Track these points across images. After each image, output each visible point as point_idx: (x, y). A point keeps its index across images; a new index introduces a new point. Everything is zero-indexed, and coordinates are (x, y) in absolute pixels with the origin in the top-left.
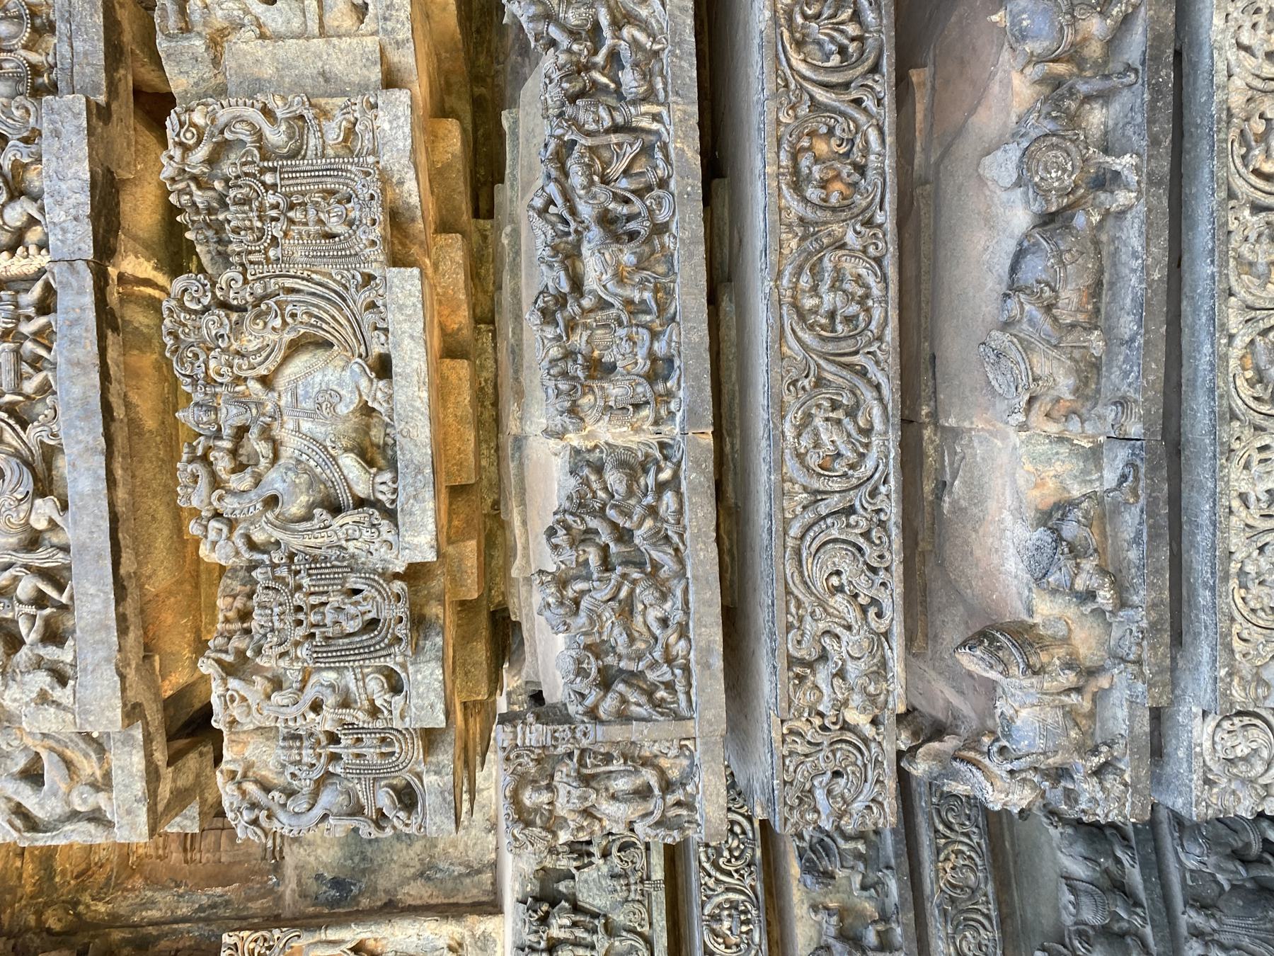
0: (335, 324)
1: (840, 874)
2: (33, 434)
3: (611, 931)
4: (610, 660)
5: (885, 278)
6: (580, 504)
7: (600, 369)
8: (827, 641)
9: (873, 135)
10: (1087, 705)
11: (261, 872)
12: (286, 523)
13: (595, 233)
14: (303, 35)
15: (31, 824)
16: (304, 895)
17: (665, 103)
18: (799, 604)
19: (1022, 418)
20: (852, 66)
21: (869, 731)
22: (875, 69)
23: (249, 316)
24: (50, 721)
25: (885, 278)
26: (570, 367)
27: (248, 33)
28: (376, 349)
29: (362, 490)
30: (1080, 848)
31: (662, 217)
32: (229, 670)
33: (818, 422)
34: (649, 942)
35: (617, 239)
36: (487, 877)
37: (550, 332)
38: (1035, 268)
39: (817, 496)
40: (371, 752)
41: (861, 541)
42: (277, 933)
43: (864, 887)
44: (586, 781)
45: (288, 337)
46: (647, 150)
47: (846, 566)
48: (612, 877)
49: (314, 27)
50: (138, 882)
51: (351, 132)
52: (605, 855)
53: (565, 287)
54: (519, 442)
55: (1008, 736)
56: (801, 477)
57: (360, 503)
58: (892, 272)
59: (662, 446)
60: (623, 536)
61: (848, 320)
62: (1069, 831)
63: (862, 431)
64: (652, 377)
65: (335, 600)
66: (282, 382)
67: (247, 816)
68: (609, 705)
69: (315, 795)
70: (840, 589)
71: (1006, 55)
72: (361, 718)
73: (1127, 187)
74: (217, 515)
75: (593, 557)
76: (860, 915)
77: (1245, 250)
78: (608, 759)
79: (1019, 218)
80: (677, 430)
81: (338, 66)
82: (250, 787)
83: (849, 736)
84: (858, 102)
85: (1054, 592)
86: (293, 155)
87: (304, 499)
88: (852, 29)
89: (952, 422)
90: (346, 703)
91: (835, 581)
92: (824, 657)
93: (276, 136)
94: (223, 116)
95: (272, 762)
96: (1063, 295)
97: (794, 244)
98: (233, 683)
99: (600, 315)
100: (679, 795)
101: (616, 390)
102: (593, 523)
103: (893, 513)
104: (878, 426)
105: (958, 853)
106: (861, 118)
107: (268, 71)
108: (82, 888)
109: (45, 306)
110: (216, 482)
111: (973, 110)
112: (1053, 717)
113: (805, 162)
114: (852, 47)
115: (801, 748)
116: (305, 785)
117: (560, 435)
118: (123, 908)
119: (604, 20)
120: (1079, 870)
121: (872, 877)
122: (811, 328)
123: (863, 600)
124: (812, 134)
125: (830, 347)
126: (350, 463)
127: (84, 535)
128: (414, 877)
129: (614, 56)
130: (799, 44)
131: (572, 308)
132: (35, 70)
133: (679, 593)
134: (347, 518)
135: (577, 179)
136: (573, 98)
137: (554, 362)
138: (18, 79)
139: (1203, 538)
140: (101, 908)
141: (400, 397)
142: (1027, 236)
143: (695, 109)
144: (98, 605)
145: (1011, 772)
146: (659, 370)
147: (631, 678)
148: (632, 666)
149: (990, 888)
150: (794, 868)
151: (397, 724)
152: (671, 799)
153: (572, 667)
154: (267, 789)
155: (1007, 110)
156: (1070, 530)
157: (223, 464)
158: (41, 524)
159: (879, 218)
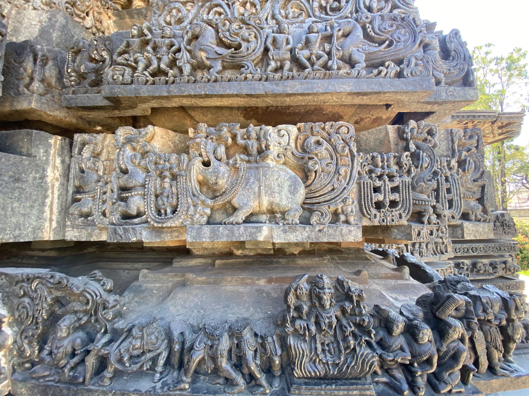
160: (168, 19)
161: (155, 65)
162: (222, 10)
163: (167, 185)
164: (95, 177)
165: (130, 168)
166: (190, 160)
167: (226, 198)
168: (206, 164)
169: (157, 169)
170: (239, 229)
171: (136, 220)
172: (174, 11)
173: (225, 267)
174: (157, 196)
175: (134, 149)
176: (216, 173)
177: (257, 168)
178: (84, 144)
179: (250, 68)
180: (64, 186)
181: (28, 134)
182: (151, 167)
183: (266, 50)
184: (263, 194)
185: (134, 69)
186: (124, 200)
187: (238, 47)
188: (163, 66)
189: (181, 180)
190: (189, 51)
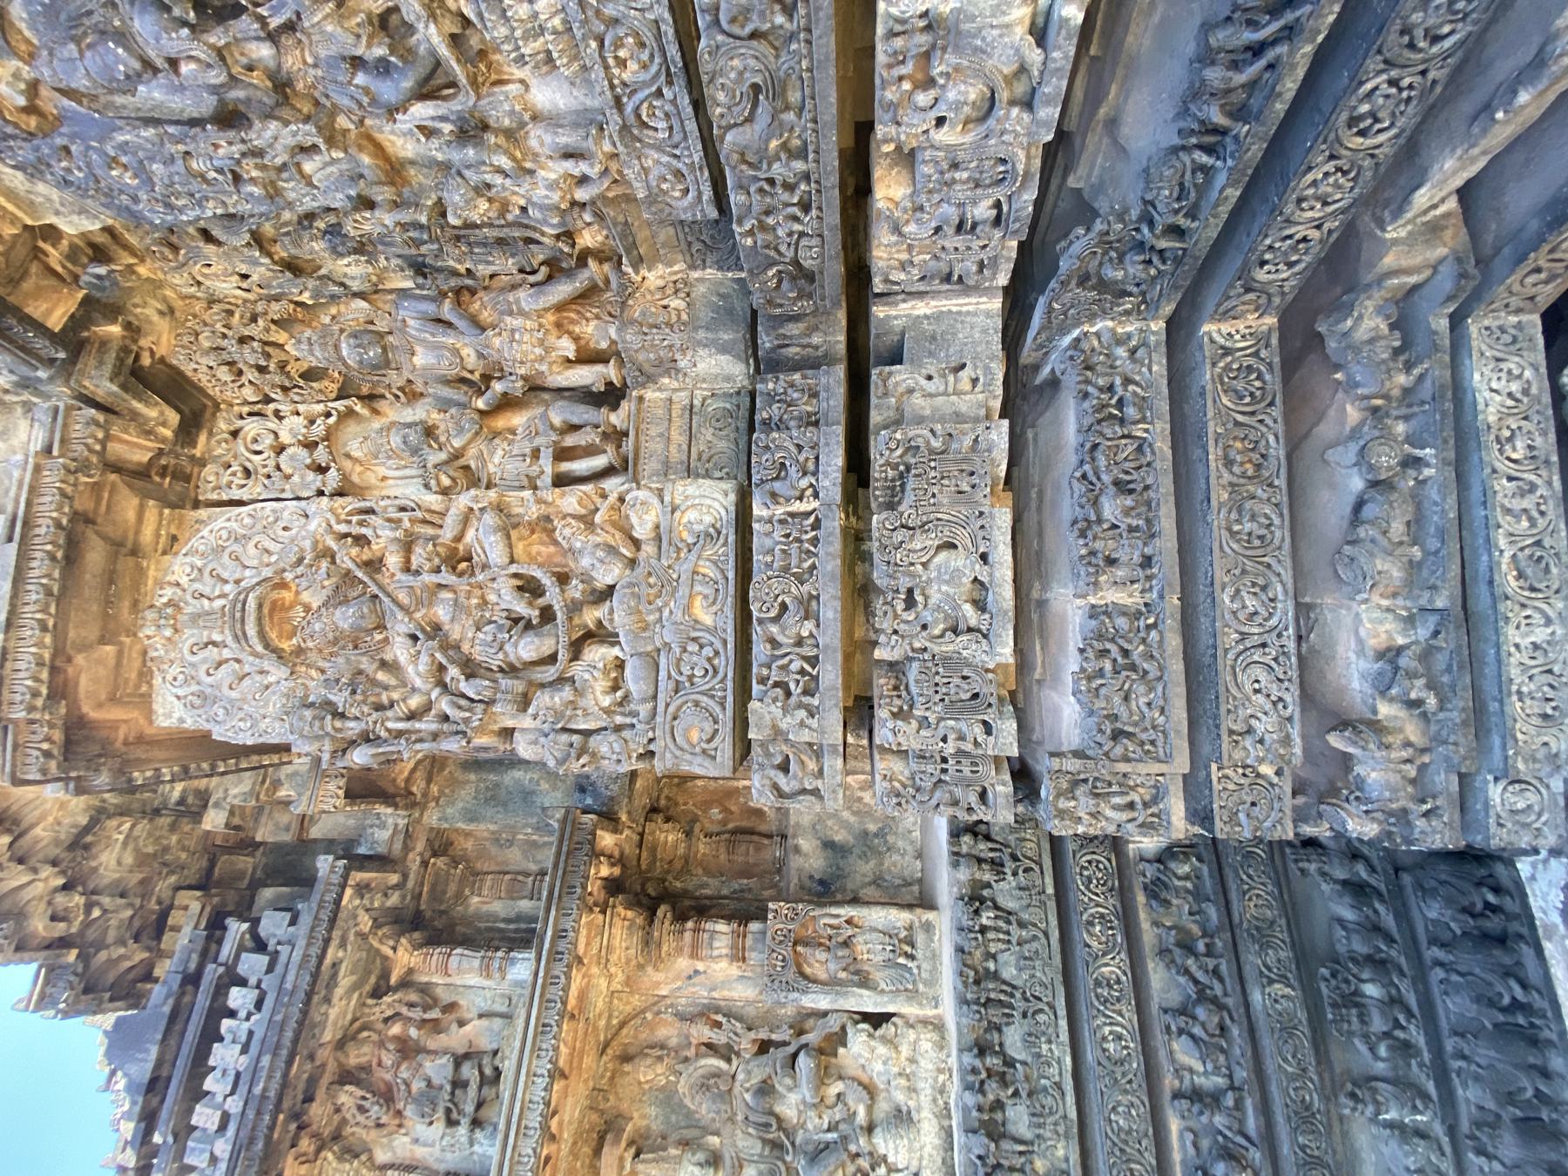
0: (962, 537)
1: (1175, 901)
2: (805, 588)
3: (1022, 925)
4: (1119, 725)
5: (1281, 515)
6: (1100, 637)
7: (1111, 562)
8: (1253, 722)
9: (1271, 439)
10: (1413, 773)
11: (769, 872)
12: (933, 638)
13: (1112, 490)
14: (945, 394)
15: (781, 794)
16: (802, 888)
17: (1151, 423)
18: (1235, 698)
19: (1365, 596)
20: (1259, 402)
21: (1275, 780)
22: (1271, 404)
23: (918, 531)
24: (806, 736)
25: (1281, 515)
26: (1094, 561)
27: (917, 394)
28: (982, 550)
29: (973, 623)
30: (1348, 899)
31: (1149, 481)
32: (895, 715)
33: (1244, 593)
34: (1046, 934)
35: (1123, 492)
36: (916, 888)
37: (1081, 542)
38: (1369, 511)
39: (1244, 636)
40: (967, 770)
41: (1273, 664)
42: (800, 906)
43: (1191, 914)
44: (1097, 795)
45: (937, 543)
46: (1140, 449)
47: (1263, 676)
48: (1020, 889)
49: (950, 390)
50: (700, 871)
51: (976, 440)
52: (1015, 874)
53: (1093, 517)
54: (1042, 604)
55: (1361, 789)
56: (1234, 624)
57: (970, 630)
58: (1286, 512)
59: (1146, 605)
60: (1126, 653)
61: (1261, 538)
62: (1338, 887)
63: (1272, 600)
64: (1142, 566)
65: (957, 681)
66: (932, 566)
67: (895, 800)
68: (1118, 750)
69: (932, 791)
70: (1257, 691)
71: (1340, 395)
72: (969, 747)
73: (1428, 465)
74: (895, 632)
75: (1108, 666)
76: (1188, 932)
77: (1506, 502)
78: (1110, 785)
79: (1357, 484)
80: (1155, 595)
81: (964, 409)
82: (896, 784)
83: (1260, 781)
84: (1261, 421)
85: (1392, 700)
86: (942, 453)
87: (942, 626)
88: (1257, 384)
89: (1307, 599)
90: (962, 738)
91: (1256, 686)
92: (1250, 731)
93: (936, 444)
94: (911, 434)
95: (907, 773)
96: (1394, 525)
97: (1226, 496)
98: (899, 723)
99: (1111, 533)
100: (1154, 810)
101: (1120, 573)
102: (1108, 646)
103: (1291, 646)
104: (1280, 597)
105: (1258, 896)
106: (1264, 430)
107: (928, 412)
108: (668, 872)
109: (816, 526)
110: (896, 616)
111: (1316, 424)
112: (1394, 778)
113: (1232, 454)
114: (1258, 393)
115: (1231, 787)
116: (928, 784)
117: (1084, 596)
118: (690, 887)
119: (1118, 381)
120: (1349, 915)
121: (1195, 908)
122: (1238, 541)
123: (1274, 698)
124: (1235, 438)
125: (1249, 553)
126: (968, 609)
127: (828, 640)
128: (870, 884)
129: (1121, 400)
130: (1225, 391)
131: (1097, 529)
132: (809, 414)
133: (1160, 689)
134: (964, 638)
135: (1102, 461)
136: (1099, 422)
137: (1082, 557)
138: (801, 419)
139: (1489, 671)
140: (678, 884)
141: (997, 574)
142: (1364, 492)
143: (1168, 426)
144: (832, 676)
145: (1367, 812)
146: (1147, 562)
147: (1129, 735)
148: (1131, 729)
149: (1283, 922)
150: (1141, 898)
151: (990, 752)
152: (1150, 811)
153: (1095, 727)
154: (905, 787)
155: (1342, 422)
156: (1403, 662)
157: (900, 606)
158: (805, 634)
159: (1276, 483)
160: (677, 194)
161: (796, 210)
162: (645, 105)
163: (965, 175)
164: (933, 263)
165: (934, 224)
166: (932, 146)
167: (1000, 84)
168: (940, 121)
169: (940, 191)
170: (1055, 60)
171: (1005, 208)
172: (664, 186)
173: (1108, 35)
174: (977, 186)
175: (908, 221)
176: (958, 105)
177: (959, 33)
178: (887, 281)
179: (792, 63)
180: (935, 294)
181: (878, 336)
182: (936, 197)
183: (754, 35)
184: (1006, 19)
185: (802, 234)
186: (974, 226)
187: (756, 88)
188: (795, 201)
189: (961, 156)
190: (770, 165)
